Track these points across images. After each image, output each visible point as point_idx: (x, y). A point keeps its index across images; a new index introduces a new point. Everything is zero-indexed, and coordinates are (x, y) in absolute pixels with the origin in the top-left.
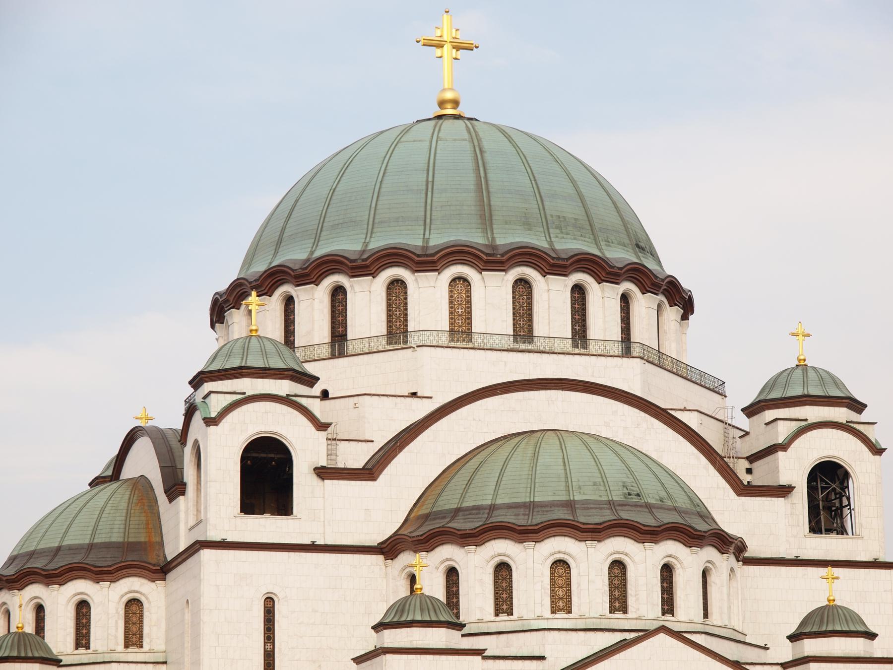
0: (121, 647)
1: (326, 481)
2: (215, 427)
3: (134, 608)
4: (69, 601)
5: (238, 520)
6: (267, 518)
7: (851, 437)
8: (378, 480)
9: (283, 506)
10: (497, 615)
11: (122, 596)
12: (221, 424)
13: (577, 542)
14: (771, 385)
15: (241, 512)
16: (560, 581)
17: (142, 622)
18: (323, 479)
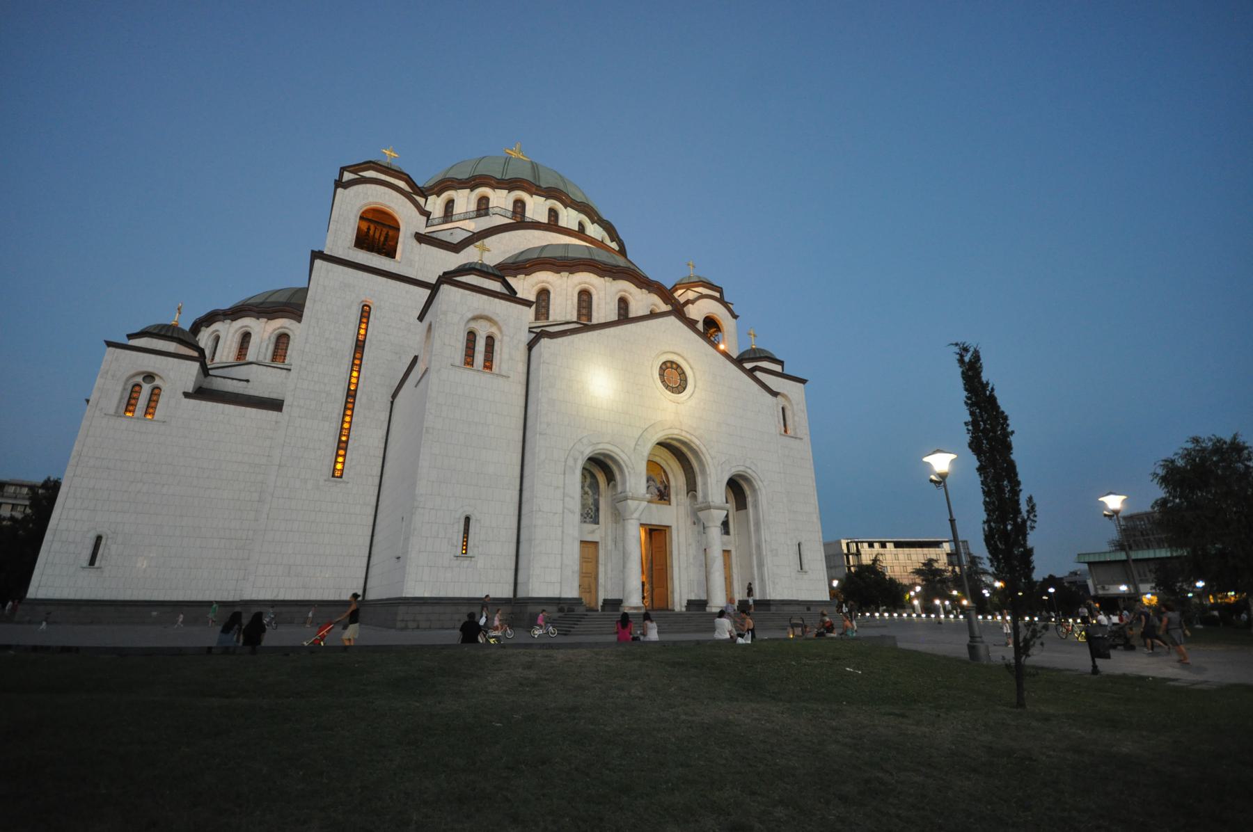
0: (268, 360)
1: (422, 244)
2: (343, 190)
3: (282, 341)
4: (236, 331)
5: (351, 251)
6: (373, 255)
7: (722, 306)
8: (460, 254)
9: (391, 253)
10: (535, 320)
11: (275, 330)
12: (348, 190)
13: (599, 278)
14: (682, 280)
15: (355, 246)
16: (584, 304)
17: (286, 349)
18: (420, 243)
